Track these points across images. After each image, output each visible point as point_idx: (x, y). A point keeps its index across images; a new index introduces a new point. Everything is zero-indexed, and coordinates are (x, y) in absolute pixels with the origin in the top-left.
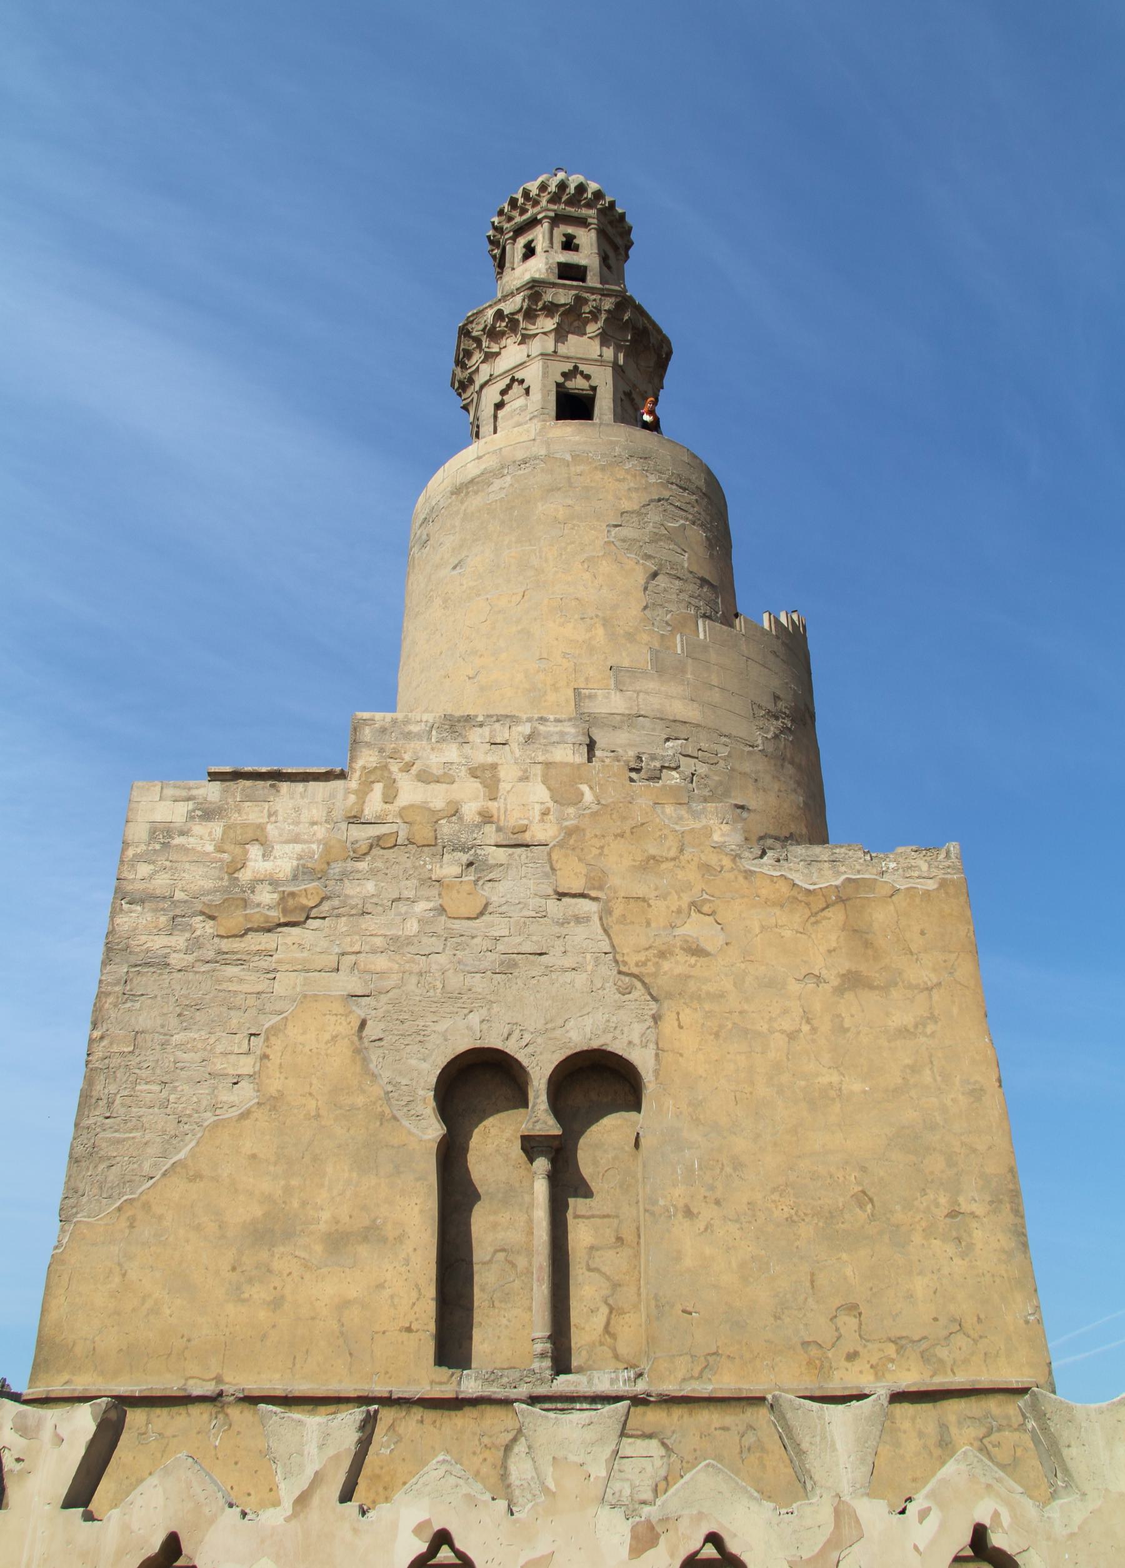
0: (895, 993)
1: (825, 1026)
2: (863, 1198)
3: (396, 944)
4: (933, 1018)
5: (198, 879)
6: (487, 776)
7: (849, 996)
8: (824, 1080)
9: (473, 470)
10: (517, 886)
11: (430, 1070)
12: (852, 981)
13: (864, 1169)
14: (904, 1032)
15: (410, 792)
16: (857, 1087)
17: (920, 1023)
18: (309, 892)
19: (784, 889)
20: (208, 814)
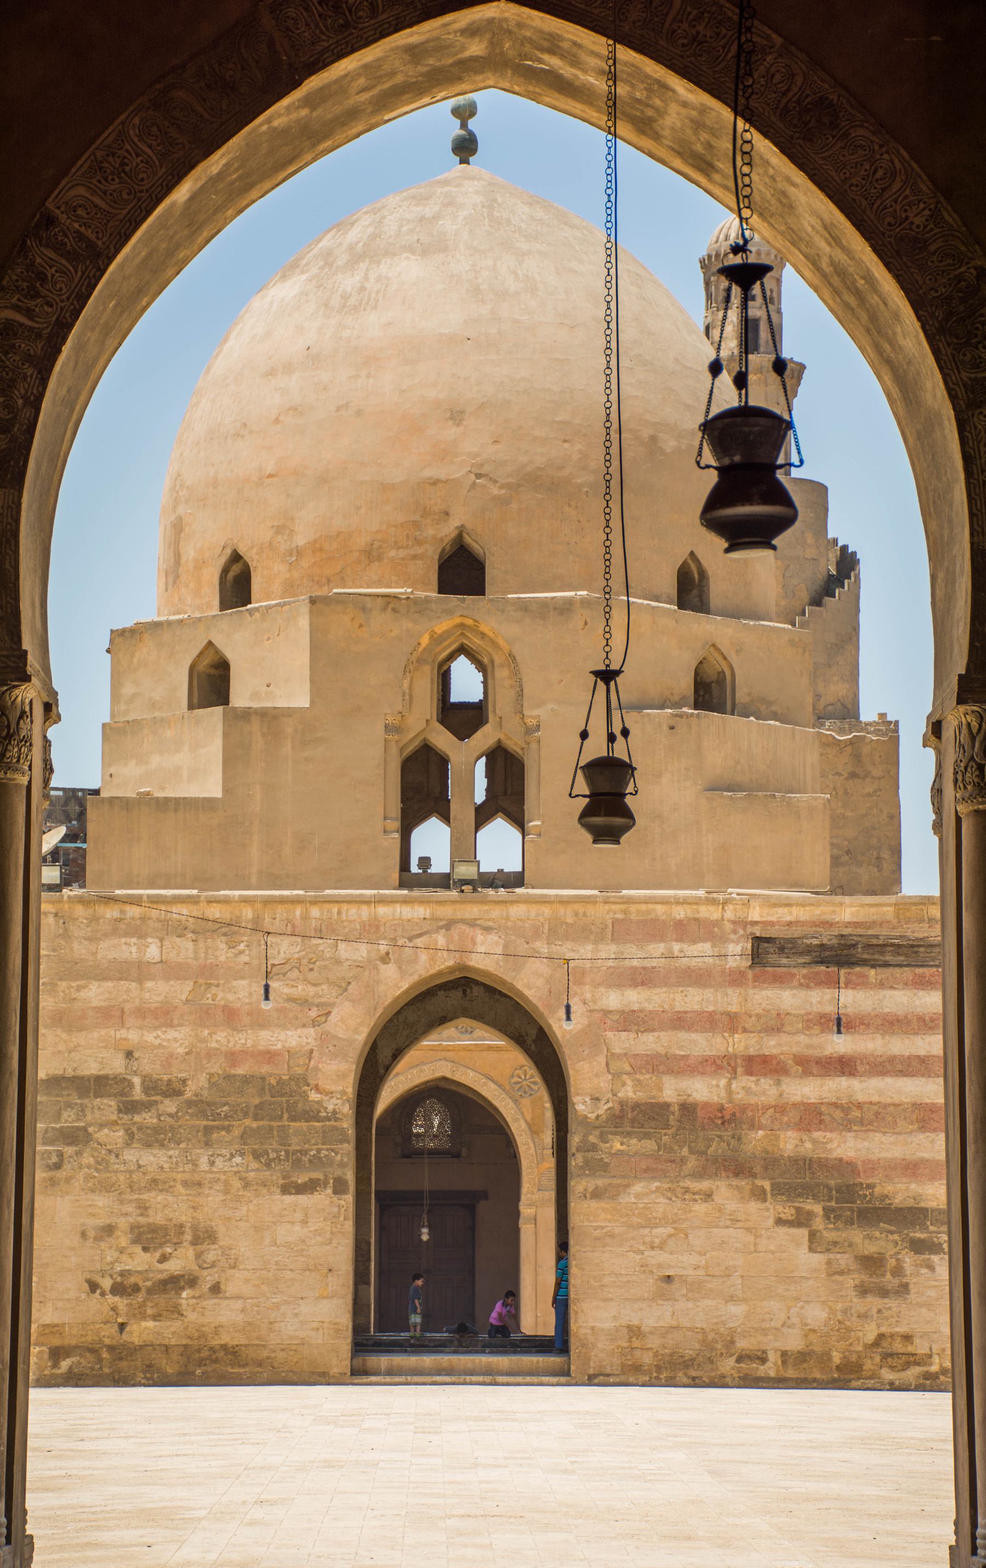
0: (867, 780)
1: (841, 792)
2: (848, 852)
4: (880, 790)
7: (851, 781)
8: (838, 812)
12: (853, 775)
13: (849, 842)
14: (869, 795)
16: (850, 814)
17: (875, 791)
19: (831, 739)
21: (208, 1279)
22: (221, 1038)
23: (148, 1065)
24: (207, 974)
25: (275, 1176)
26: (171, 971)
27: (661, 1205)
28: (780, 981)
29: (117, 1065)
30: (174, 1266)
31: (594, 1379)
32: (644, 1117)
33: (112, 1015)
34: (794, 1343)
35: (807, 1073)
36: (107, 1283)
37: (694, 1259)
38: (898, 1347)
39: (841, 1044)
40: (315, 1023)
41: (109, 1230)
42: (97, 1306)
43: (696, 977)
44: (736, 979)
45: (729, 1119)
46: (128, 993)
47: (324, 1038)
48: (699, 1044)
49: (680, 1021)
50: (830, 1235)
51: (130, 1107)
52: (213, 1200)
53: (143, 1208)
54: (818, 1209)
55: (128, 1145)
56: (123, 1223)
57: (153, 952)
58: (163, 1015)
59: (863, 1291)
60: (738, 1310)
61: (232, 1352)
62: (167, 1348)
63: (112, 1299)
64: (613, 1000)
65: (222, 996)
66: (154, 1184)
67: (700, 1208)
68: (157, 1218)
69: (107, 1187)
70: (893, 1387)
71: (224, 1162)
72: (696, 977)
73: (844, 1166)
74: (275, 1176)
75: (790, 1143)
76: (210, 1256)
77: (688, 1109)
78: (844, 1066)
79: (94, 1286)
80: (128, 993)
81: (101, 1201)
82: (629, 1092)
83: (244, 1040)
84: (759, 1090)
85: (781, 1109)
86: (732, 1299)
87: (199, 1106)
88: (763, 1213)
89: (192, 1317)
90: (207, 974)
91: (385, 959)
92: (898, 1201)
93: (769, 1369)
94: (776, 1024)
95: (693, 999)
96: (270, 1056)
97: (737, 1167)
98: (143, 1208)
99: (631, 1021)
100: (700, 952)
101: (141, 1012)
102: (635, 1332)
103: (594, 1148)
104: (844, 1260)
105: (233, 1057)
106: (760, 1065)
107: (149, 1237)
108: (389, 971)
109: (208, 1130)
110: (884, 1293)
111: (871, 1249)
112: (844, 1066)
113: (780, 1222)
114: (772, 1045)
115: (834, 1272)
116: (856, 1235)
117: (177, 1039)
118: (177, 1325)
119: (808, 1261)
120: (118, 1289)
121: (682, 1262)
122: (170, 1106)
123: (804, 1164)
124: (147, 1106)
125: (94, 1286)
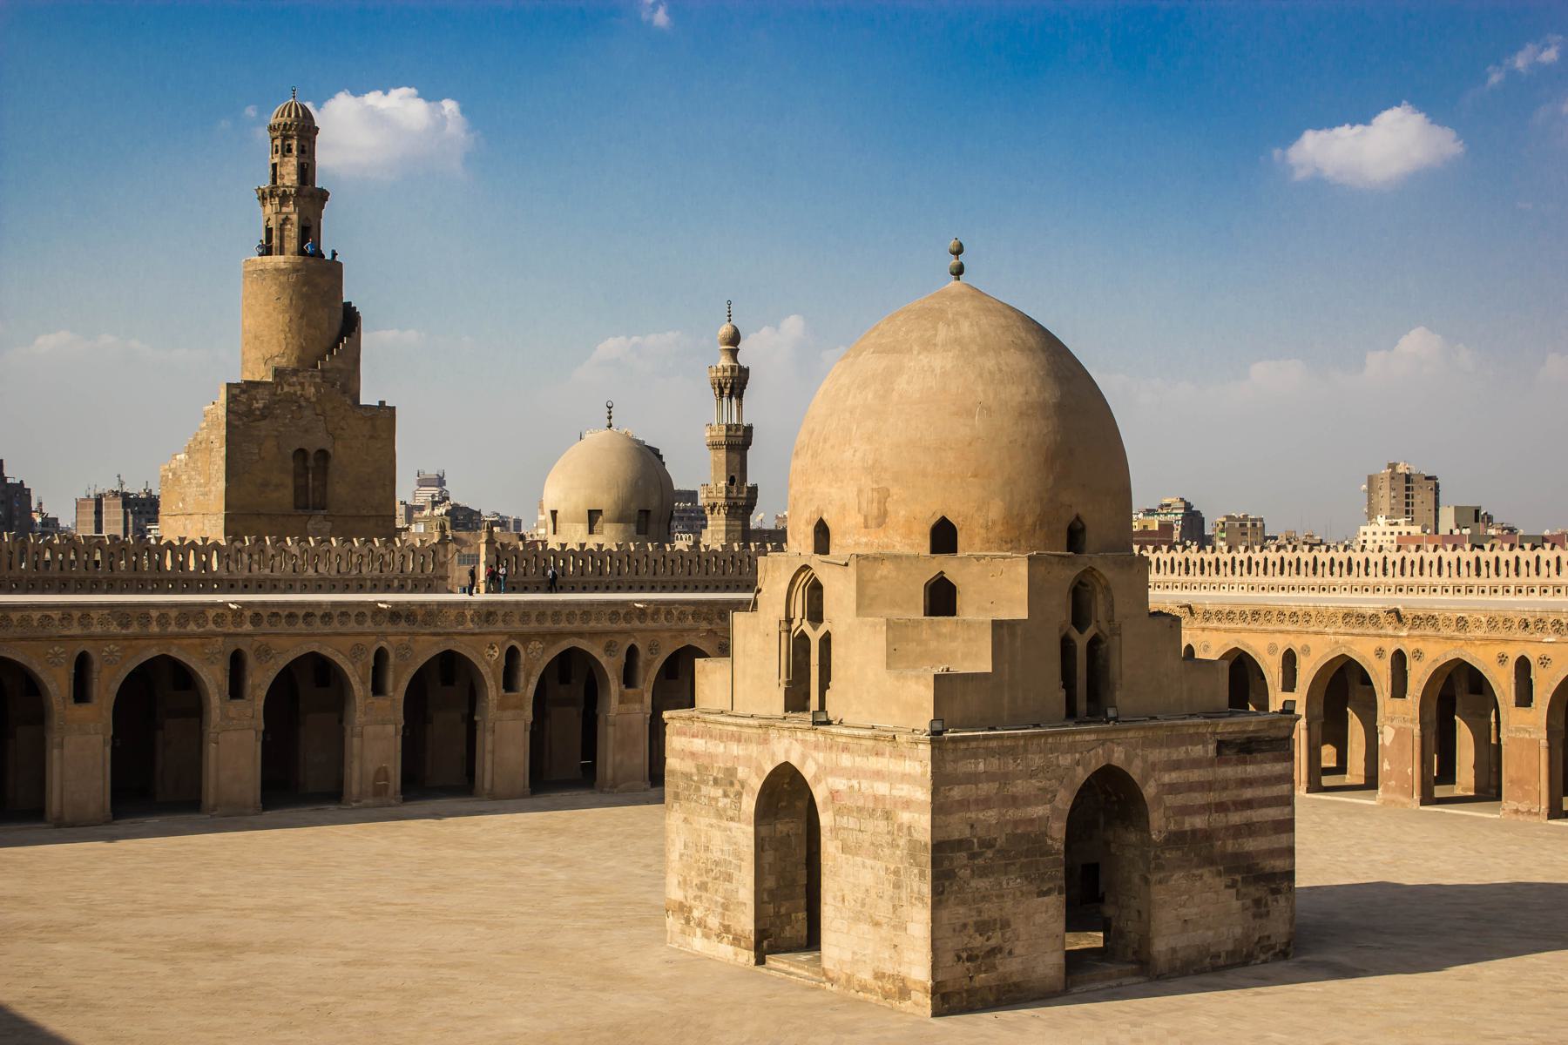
3: (284, 425)
5: (243, 408)
6: (302, 384)
9: (283, 266)
10: (308, 412)
11: (291, 452)
12: (371, 437)
15: (286, 389)
18: (266, 412)
20: (243, 392)
21: (1007, 947)
22: (1011, 814)
23: (981, 832)
24: (1004, 778)
25: (1033, 888)
26: (990, 777)
27: (1184, 884)
28: (1227, 762)
29: (967, 833)
30: (993, 942)
31: (1159, 977)
32: (1177, 839)
33: (964, 804)
34: (1230, 946)
35: (1237, 810)
36: (964, 955)
37: (1195, 910)
38: (1266, 943)
39: (1248, 793)
40: (1050, 802)
41: (965, 926)
42: (960, 969)
43: (1196, 763)
44: (1211, 763)
45: (1207, 835)
46: (969, 791)
47: (1054, 810)
48: (1198, 798)
49: (1191, 787)
50: (1243, 890)
51: (973, 856)
52: (1008, 903)
53: (980, 912)
54: (1239, 877)
55: (972, 876)
56: (971, 921)
57: (981, 767)
58: (985, 803)
59: (1255, 916)
60: (1210, 933)
61: (1017, 985)
62: (991, 988)
63: (968, 964)
64: (1167, 778)
65: (1012, 790)
66: (984, 898)
67: (1198, 884)
68: (985, 917)
69: (963, 902)
70: (1264, 962)
71: (1013, 882)
72: (1196, 763)
73: (1248, 855)
74: (1033, 888)
75: (1231, 846)
76: (1008, 935)
77: (1194, 832)
78: (1249, 804)
79: (959, 958)
80: (969, 791)
81: (961, 910)
82: (1172, 827)
83: (1020, 814)
84: (1219, 820)
85: (1227, 828)
86: (1209, 928)
87: (1003, 853)
88: (1220, 882)
89: (1001, 969)
90: (1004, 778)
91: (1078, 763)
92: (1268, 869)
93: (1221, 961)
94: (1225, 785)
95: (1196, 775)
96: (1032, 821)
97: (1209, 861)
98: (980, 912)
99: (1173, 788)
100: (1197, 751)
101: (977, 802)
102: (1174, 950)
103: (1158, 857)
104: (1248, 902)
105: (1016, 823)
106: (1221, 807)
107: (983, 927)
108: (1080, 770)
109: (1006, 865)
110: (1261, 916)
111: (1257, 895)
112: (1249, 804)
113: (1227, 887)
114: (1226, 796)
115: (1245, 908)
116: (1252, 889)
117: (991, 815)
118: (994, 975)
119: (1236, 904)
120: (969, 959)
121: (1191, 912)
122: (990, 854)
123: (1236, 856)
124: (980, 855)
125: (959, 958)
